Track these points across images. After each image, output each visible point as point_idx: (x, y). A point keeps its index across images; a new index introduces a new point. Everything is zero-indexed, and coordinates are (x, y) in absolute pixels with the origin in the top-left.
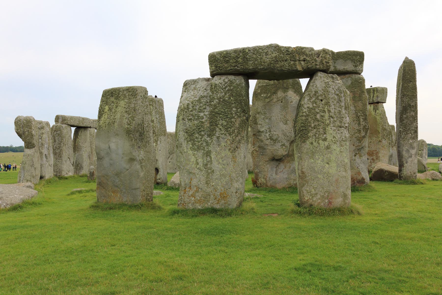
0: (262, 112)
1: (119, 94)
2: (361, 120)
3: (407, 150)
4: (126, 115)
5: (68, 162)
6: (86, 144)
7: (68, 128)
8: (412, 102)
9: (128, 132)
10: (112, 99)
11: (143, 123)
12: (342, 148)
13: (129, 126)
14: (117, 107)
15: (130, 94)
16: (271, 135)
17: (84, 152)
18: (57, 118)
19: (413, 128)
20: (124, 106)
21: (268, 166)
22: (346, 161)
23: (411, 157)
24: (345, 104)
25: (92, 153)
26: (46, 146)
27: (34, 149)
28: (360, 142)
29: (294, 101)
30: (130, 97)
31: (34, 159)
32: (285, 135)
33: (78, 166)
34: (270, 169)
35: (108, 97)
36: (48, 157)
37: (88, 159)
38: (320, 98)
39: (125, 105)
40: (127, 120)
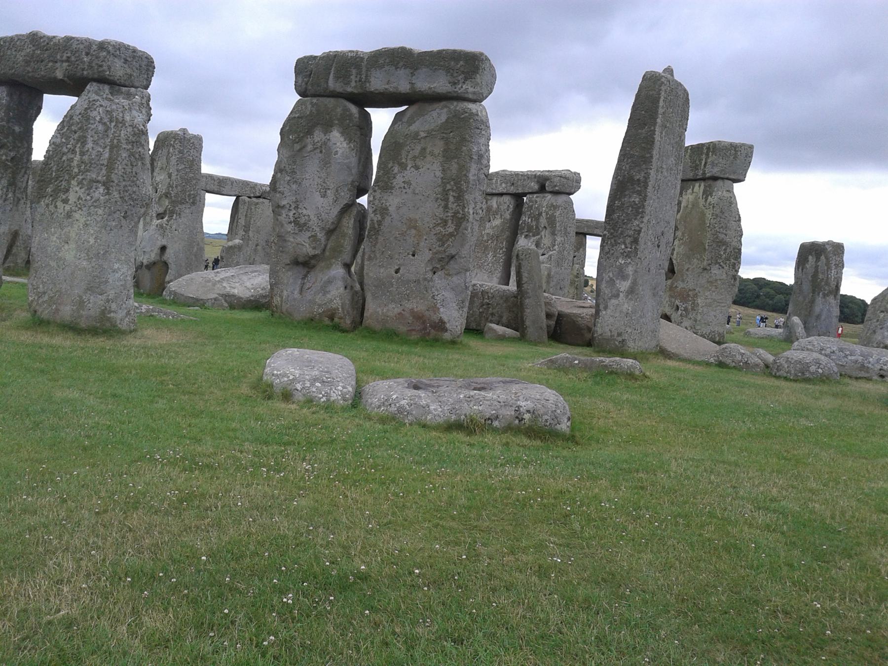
0: (288, 169)
2: (451, 199)
3: (611, 279)
8: (639, 172)
12: (89, 218)
16: (296, 216)
19: (631, 233)
21: (290, 273)
22: (92, 241)
23: (617, 296)
24: (112, 141)
28: (443, 245)
29: (340, 152)
32: (319, 216)
34: (291, 281)
38: (73, 128)
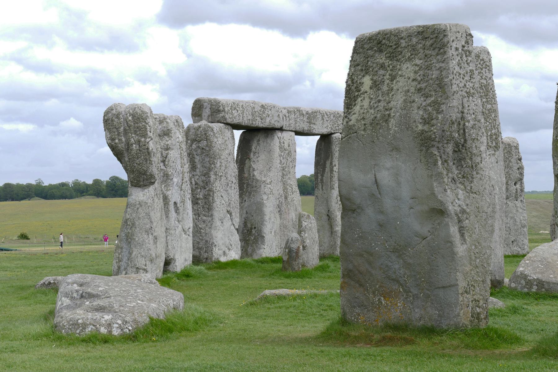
1: (398, 45)
4: (419, 100)
5: (228, 223)
6: (271, 174)
7: (227, 132)
9: (426, 142)
10: (381, 59)
11: (463, 118)
13: (426, 128)
14: (393, 78)
15: (428, 43)
17: (265, 197)
18: (198, 108)
20: (412, 75)
25: (286, 198)
26: (175, 180)
27: (151, 188)
30: (427, 52)
31: (152, 214)
33: (250, 234)
35: (370, 53)
36: (181, 209)
37: (278, 215)
39: (416, 72)
40: (421, 113)
